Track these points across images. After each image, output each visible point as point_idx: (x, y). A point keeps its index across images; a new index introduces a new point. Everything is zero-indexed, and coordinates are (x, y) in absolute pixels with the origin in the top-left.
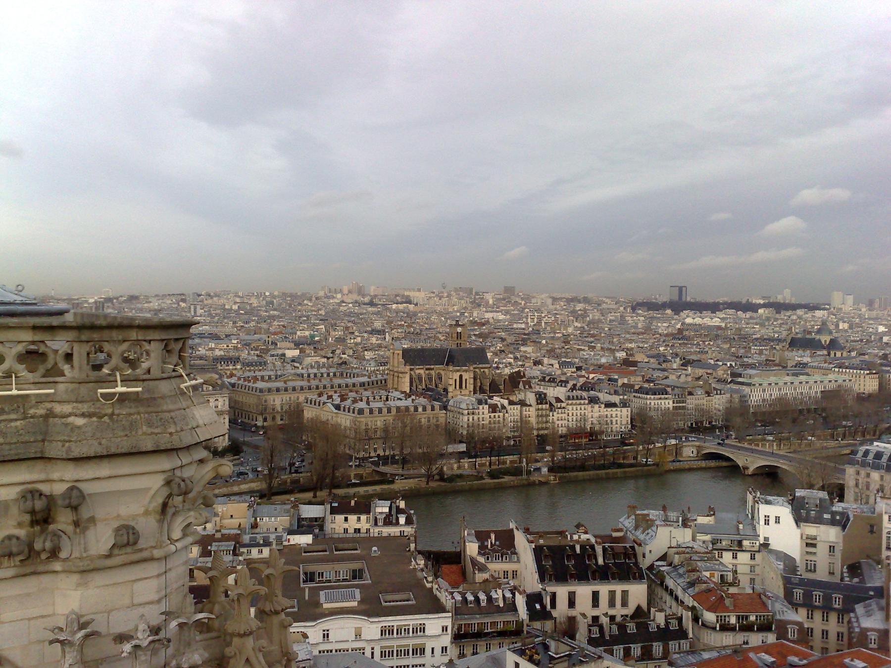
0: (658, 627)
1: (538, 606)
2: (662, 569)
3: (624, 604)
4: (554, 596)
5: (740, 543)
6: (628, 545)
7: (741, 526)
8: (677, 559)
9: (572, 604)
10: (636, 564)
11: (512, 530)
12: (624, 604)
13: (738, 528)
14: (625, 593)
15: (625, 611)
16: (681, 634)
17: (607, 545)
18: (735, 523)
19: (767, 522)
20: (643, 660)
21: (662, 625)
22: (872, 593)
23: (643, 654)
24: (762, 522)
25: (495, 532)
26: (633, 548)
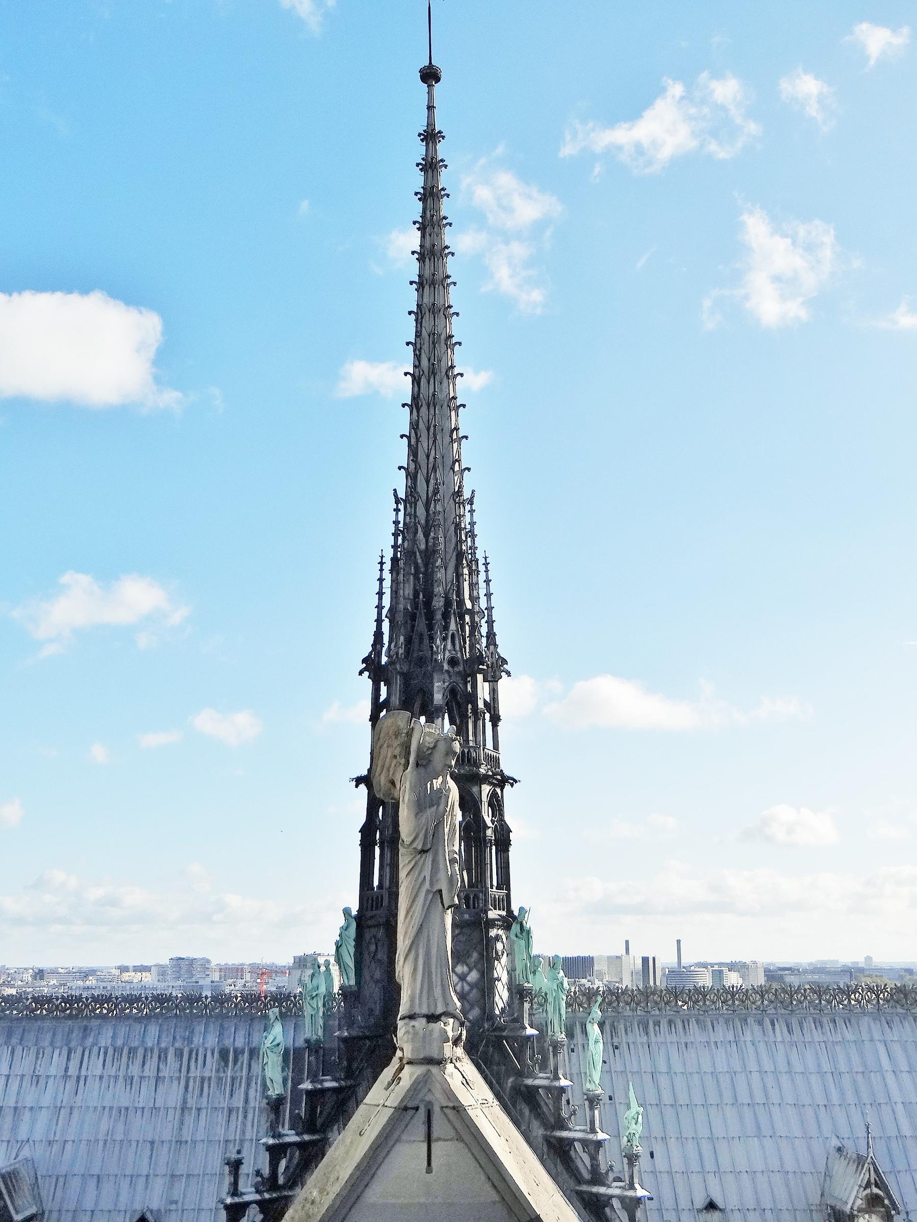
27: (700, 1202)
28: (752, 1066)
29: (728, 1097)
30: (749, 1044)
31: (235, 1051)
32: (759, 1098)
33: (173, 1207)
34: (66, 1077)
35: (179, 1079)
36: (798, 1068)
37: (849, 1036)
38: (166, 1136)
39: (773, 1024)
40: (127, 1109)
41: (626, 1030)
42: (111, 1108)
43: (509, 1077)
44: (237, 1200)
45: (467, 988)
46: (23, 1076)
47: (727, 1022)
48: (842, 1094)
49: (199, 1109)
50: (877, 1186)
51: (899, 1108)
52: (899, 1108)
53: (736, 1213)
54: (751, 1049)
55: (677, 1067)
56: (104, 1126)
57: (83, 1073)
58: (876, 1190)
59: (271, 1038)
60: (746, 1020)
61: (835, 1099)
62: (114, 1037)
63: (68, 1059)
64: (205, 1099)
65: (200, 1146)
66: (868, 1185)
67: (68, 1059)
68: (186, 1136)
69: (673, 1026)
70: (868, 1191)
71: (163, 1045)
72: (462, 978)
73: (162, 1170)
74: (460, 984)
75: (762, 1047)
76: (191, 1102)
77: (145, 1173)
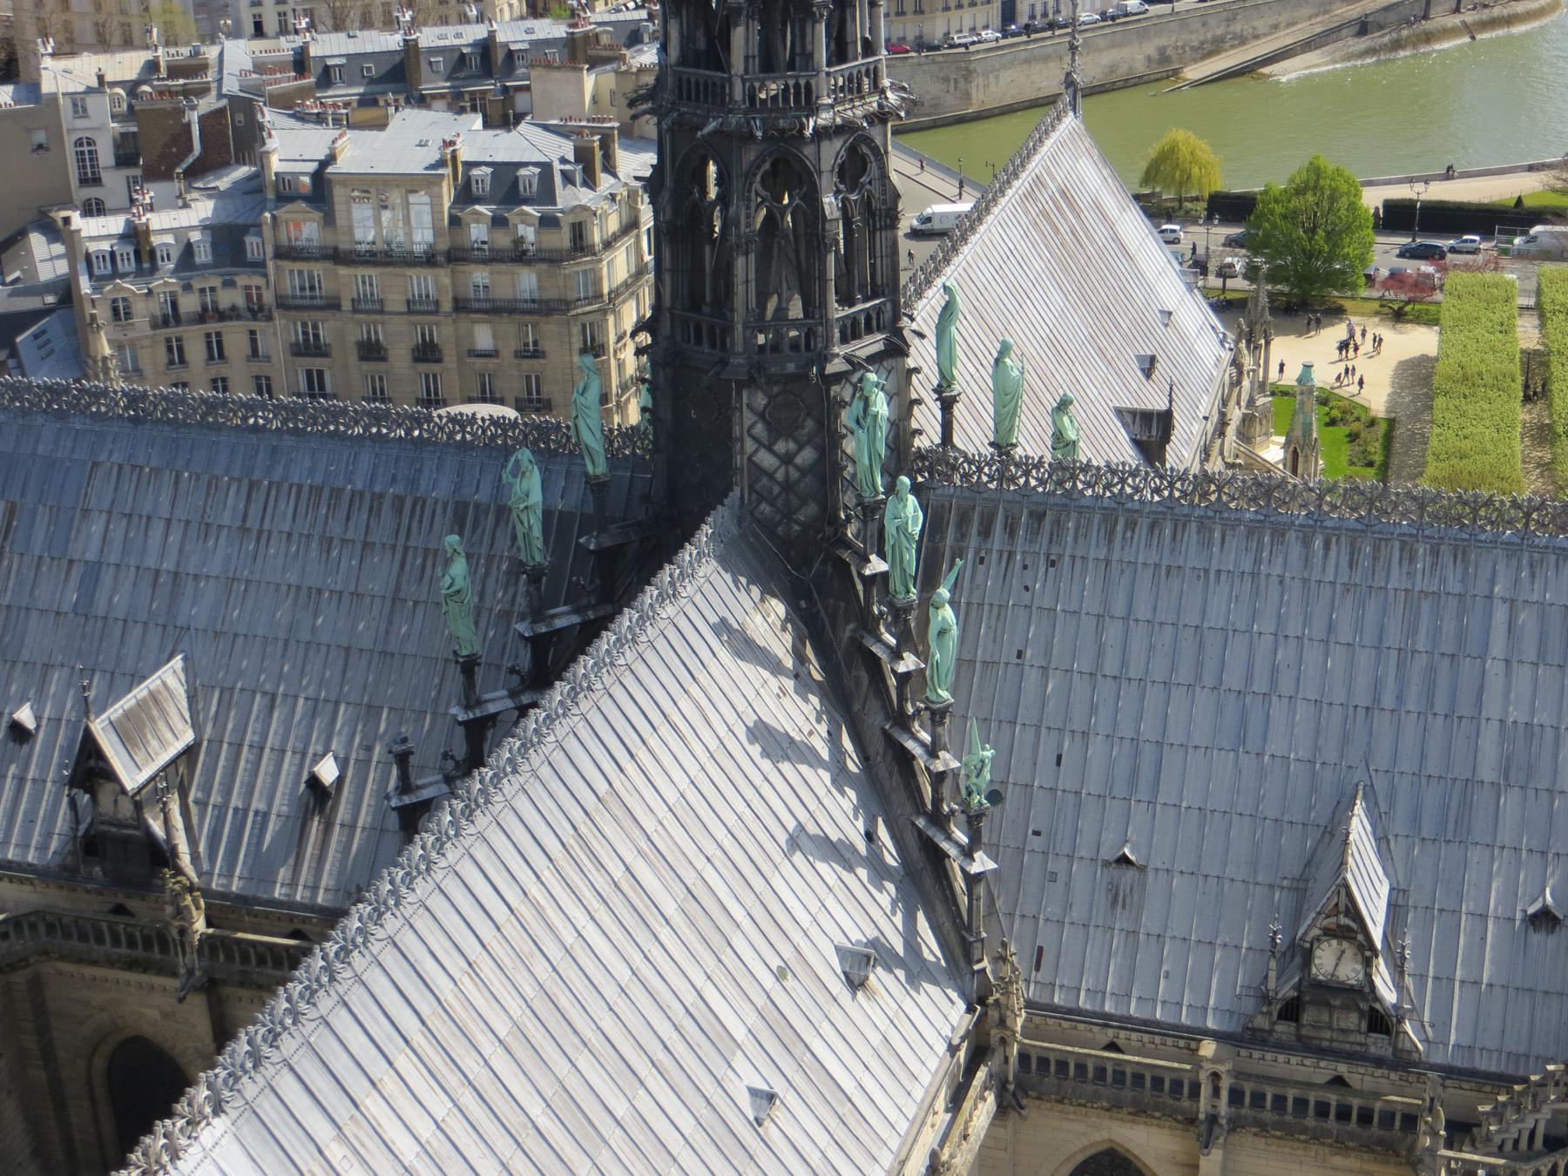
27: (1107, 853)
28: (1266, 625)
29: (1209, 680)
30: (1274, 580)
32: (1260, 685)
34: (244, 530)
35: (394, 547)
36: (1345, 633)
37: (1454, 586)
38: (366, 643)
39: (1327, 546)
41: (1076, 533)
42: (299, 588)
43: (847, 623)
44: (407, 800)
45: (794, 474)
46: (188, 522)
47: (1250, 532)
48: (1400, 698)
50: (1347, 913)
51: (1490, 733)
52: (1490, 733)
53: (1162, 875)
54: (1274, 589)
55: (1142, 610)
57: (266, 526)
58: (1344, 920)
59: (447, 581)
60: (1283, 535)
61: (1388, 701)
62: (311, 472)
63: (248, 501)
66: (1336, 910)
67: (248, 501)
68: (393, 647)
69: (1156, 532)
70: (1333, 920)
71: (378, 489)
72: (787, 459)
74: (783, 469)
75: (1294, 591)
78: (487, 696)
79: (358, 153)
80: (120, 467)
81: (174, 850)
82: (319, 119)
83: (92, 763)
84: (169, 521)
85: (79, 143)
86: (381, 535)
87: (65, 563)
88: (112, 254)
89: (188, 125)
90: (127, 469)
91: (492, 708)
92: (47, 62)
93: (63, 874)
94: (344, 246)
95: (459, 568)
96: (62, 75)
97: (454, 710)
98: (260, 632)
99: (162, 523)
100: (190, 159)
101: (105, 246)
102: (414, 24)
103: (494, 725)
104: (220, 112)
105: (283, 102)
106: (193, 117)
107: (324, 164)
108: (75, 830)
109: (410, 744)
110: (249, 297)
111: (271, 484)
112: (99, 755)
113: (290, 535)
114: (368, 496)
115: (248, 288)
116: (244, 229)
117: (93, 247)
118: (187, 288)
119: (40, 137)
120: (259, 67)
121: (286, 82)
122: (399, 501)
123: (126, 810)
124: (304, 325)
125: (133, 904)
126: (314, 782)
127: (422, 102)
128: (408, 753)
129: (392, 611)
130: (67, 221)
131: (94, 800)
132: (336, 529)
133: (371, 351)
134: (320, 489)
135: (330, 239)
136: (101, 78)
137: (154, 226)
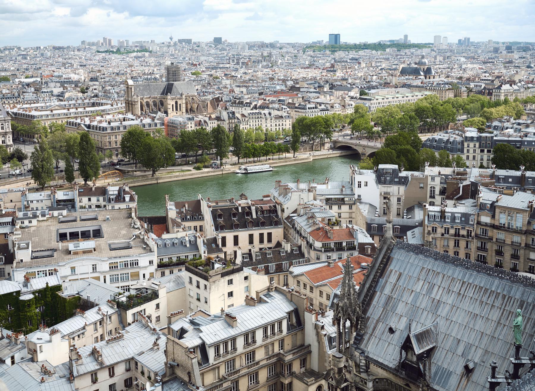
0: (286, 252)
1: (214, 245)
2: (294, 218)
3: (270, 240)
4: (224, 239)
5: (343, 199)
6: (272, 205)
7: (344, 189)
8: (302, 212)
9: (236, 242)
10: (277, 216)
11: (200, 200)
12: (270, 240)
13: (342, 190)
14: (270, 235)
15: (270, 245)
16: (302, 255)
17: (258, 206)
18: (341, 187)
19: (359, 186)
20: (277, 272)
21: (289, 251)
22: (417, 224)
23: (276, 269)
24: (357, 185)
25: (188, 202)
26: (275, 206)
31: (527, 303)
33: (483, 364)
34: (459, 294)
35: (501, 308)
38: (488, 332)
40: (477, 315)
42: (472, 313)
44: (493, 380)
46: (444, 288)
49: (505, 325)
56: (466, 320)
57: (465, 294)
62: (480, 282)
64: (508, 322)
65: (500, 341)
68: (496, 335)
71: (498, 291)
73: (482, 346)
76: (502, 321)
77: (476, 345)
78: (522, 358)
79: (506, 201)
80: (430, 270)
81: (425, 374)
82: (495, 191)
83: (408, 344)
84: (440, 287)
85: (431, 187)
86: (498, 303)
87: (411, 291)
88: (435, 216)
89: (460, 187)
90: (431, 271)
91: (523, 362)
92: (427, 167)
93: (395, 371)
94: (497, 224)
95: (520, 319)
96: (430, 171)
97: (511, 359)
98: (459, 322)
99: (438, 287)
100: (459, 196)
101: (433, 213)
102: (526, 170)
103: (523, 367)
104: (468, 185)
105: (486, 185)
106: (461, 185)
107: (494, 202)
108: (400, 360)
109: (497, 365)
110: (468, 232)
111: (469, 283)
112: (411, 343)
113: (471, 298)
114: (495, 293)
115: (468, 230)
116: (470, 215)
117: (430, 213)
118: (452, 227)
119: (422, 185)
120: (481, 176)
121: (487, 180)
122: (504, 297)
123: (415, 359)
124: (482, 243)
125: (411, 385)
126: (466, 367)
127: (524, 190)
128: (496, 367)
129: (497, 326)
130: (425, 206)
131: (407, 354)
132: (485, 299)
133: (499, 253)
134: (482, 288)
135: (493, 222)
136: (439, 173)
137: (446, 211)
